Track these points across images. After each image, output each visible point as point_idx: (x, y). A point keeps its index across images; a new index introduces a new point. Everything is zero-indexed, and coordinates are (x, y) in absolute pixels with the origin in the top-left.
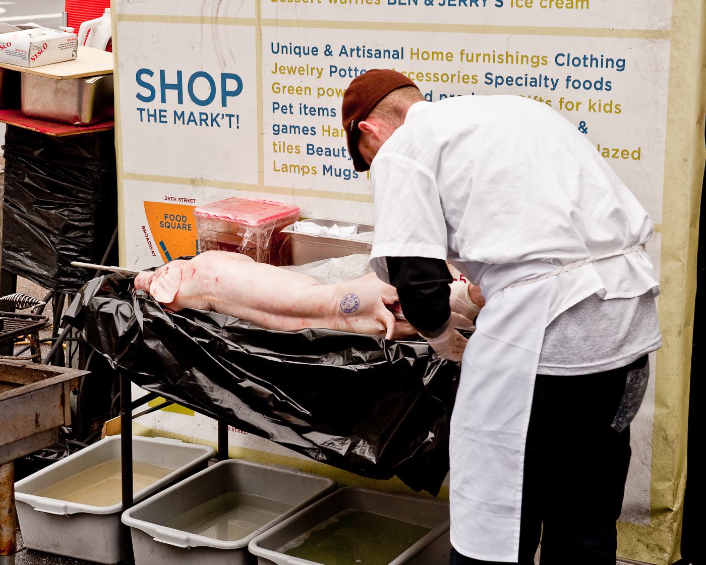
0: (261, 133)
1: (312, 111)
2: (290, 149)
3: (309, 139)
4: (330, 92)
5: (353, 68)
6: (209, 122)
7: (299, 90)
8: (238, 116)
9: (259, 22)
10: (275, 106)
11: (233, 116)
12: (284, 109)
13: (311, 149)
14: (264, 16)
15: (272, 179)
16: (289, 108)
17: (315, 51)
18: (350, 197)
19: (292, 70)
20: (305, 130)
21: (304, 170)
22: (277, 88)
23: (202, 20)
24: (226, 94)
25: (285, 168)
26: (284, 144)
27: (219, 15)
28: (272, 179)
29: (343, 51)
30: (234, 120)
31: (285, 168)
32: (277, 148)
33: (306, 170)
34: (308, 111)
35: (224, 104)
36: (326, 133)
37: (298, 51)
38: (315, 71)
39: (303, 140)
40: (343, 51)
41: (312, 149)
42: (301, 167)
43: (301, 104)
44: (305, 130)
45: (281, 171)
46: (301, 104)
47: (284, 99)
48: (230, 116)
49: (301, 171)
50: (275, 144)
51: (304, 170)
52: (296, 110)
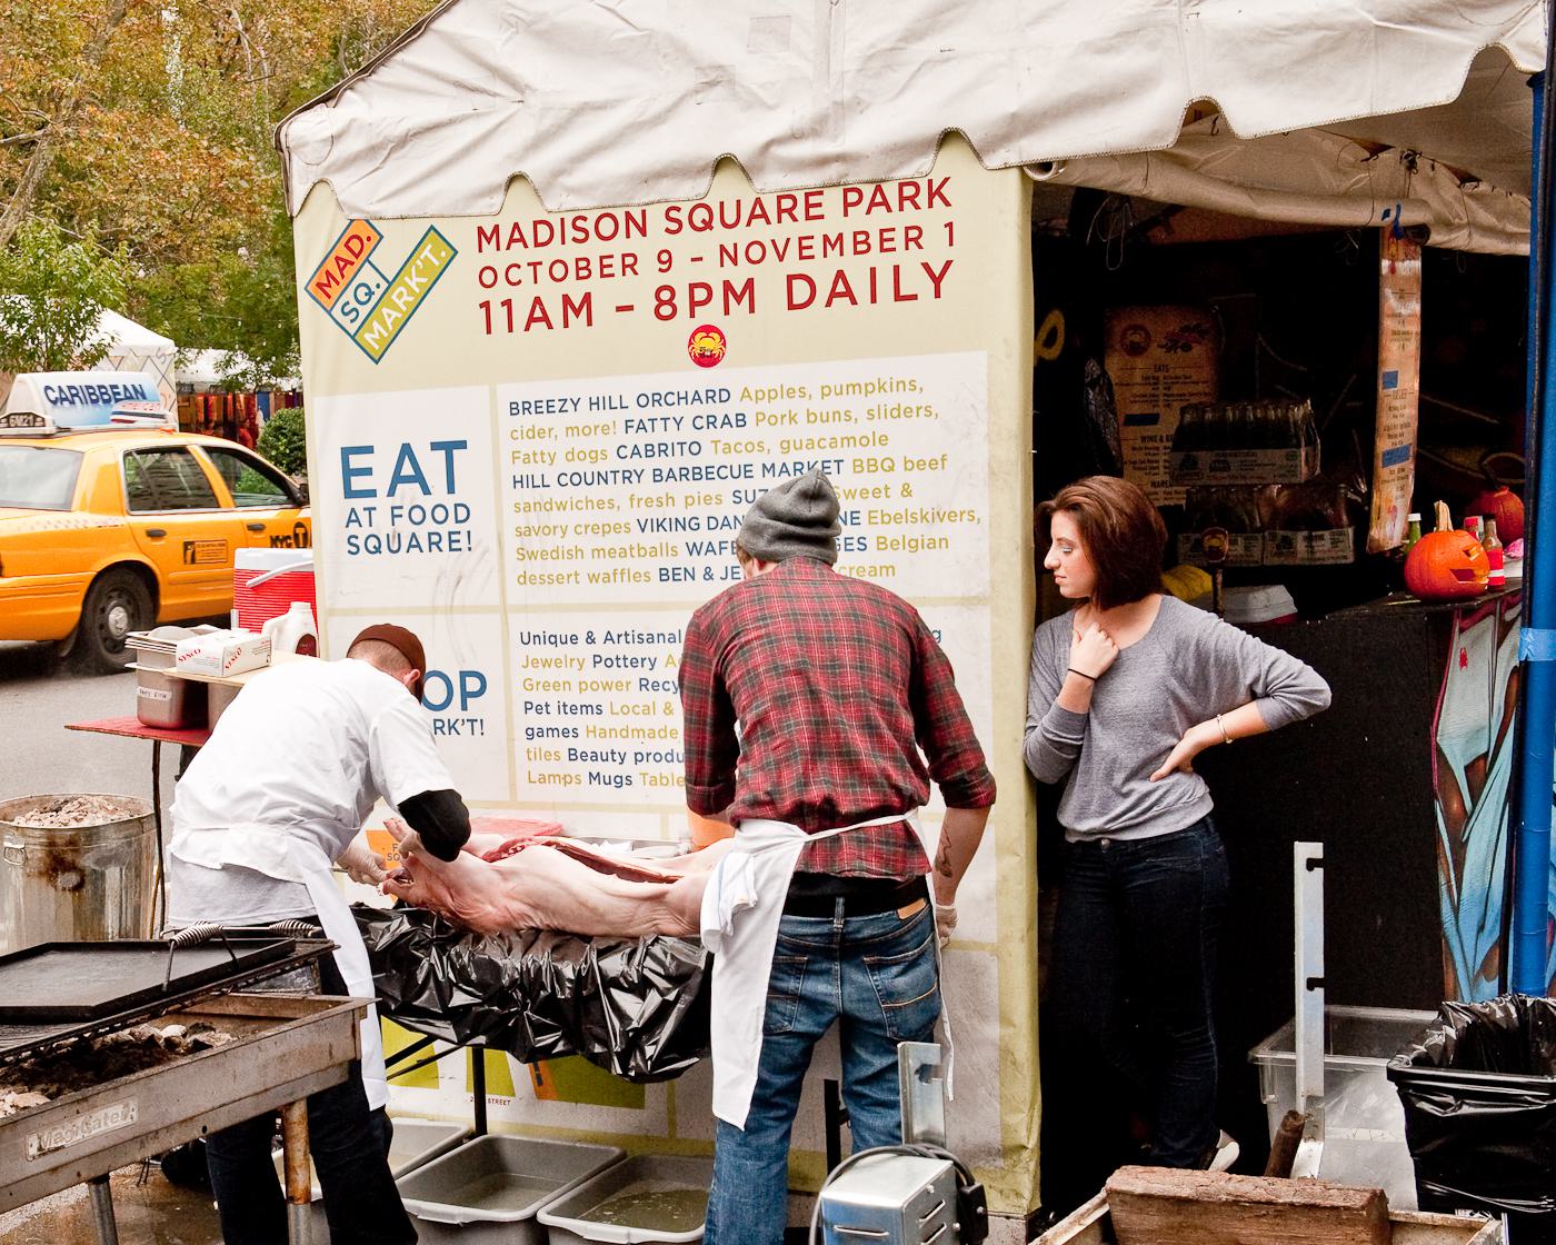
0: (511, 740)
1: (574, 709)
2: (547, 756)
3: (570, 742)
4: (595, 686)
6: (446, 729)
7: (556, 686)
9: (504, 610)
10: (528, 706)
12: (539, 709)
13: (573, 754)
14: (511, 601)
15: (526, 792)
17: (574, 639)
19: (546, 663)
20: (565, 733)
21: (566, 780)
22: (528, 685)
23: (434, 610)
24: (465, 695)
25: (543, 779)
27: (455, 603)
28: (526, 792)
29: (609, 637)
30: (477, 725)
31: (543, 779)
32: (532, 756)
33: (568, 779)
34: (568, 709)
35: (464, 707)
36: (591, 734)
37: (554, 640)
38: (575, 663)
39: (562, 745)
40: (609, 637)
44: (565, 733)
47: (538, 698)
48: (472, 721)
50: (528, 752)
51: (566, 780)
52: (553, 709)
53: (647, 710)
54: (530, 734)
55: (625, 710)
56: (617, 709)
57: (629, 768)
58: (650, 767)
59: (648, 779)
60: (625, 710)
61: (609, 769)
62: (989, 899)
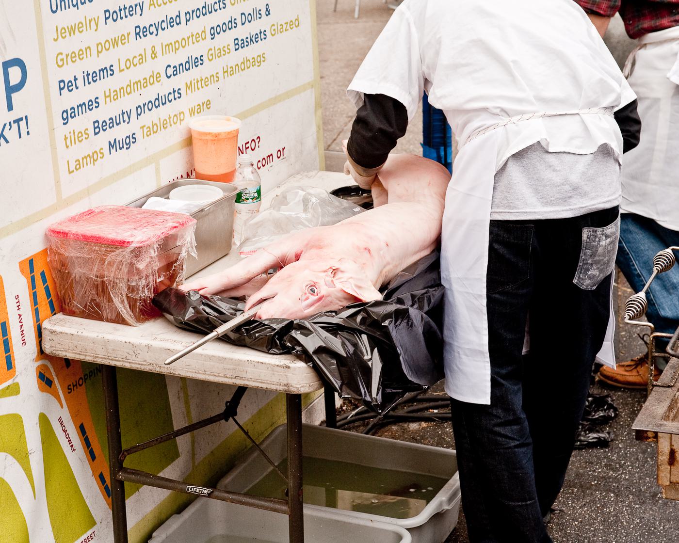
5: (122, 7)
8: (26, 117)
11: (21, 119)
16: (74, 83)
18: (132, 169)
21: (93, 157)
26: (74, 133)
31: (79, 165)
41: (98, 127)
42: (91, 155)
43: (84, 73)
45: (75, 171)
46: (84, 73)
48: (17, 121)
49: (92, 160)
50: (66, 138)
51: (93, 157)
53: (142, 58)
54: (67, 116)
55: (130, 63)
56: (123, 66)
57: (133, 126)
58: (148, 118)
59: (145, 130)
60: (130, 63)
61: (119, 133)
62: (315, 147)
